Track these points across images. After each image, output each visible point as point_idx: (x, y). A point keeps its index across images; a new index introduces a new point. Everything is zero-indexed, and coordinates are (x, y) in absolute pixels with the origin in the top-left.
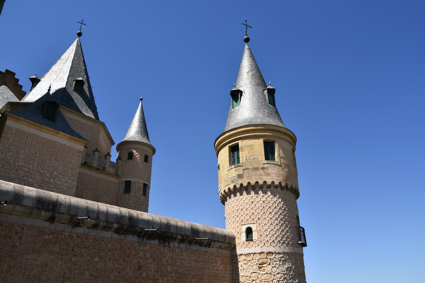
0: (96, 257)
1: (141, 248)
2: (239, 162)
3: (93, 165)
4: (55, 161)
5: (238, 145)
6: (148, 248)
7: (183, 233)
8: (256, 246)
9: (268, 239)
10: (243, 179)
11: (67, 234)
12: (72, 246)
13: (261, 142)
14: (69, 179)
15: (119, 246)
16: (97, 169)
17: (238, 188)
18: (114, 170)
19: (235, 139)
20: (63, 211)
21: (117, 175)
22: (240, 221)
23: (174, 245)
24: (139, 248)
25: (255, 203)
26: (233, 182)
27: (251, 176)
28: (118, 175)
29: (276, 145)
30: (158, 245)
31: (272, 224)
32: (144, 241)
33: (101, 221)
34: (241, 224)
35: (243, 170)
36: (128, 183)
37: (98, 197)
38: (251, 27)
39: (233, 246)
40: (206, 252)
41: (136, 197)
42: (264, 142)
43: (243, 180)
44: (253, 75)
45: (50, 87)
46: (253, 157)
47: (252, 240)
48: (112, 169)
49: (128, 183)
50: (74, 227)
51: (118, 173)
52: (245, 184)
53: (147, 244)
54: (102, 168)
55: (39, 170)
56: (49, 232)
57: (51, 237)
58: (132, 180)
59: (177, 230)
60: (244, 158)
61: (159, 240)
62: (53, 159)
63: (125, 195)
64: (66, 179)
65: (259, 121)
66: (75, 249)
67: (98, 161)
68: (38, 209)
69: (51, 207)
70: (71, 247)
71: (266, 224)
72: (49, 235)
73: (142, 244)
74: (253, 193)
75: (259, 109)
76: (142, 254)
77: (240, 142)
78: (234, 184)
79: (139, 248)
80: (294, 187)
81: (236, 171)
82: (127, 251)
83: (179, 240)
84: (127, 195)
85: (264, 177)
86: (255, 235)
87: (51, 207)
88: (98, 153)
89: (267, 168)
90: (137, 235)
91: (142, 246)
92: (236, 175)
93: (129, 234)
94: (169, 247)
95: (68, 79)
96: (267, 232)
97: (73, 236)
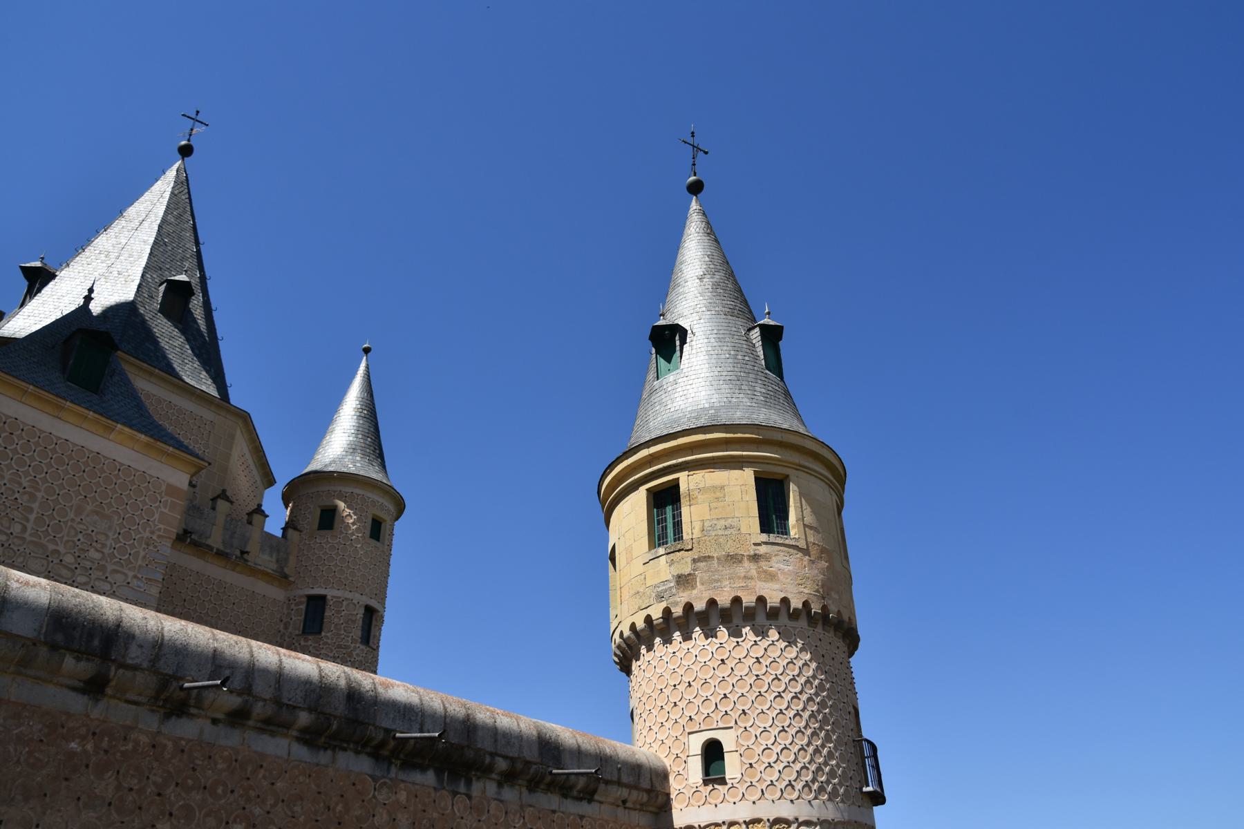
0: (235, 821)
1: (381, 798)
2: (678, 535)
3: (209, 542)
4: (96, 517)
5: (677, 486)
6: (402, 796)
7: (513, 753)
8: (737, 800)
9: (774, 778)
10: (693, 588)
11: (144, 739)
12: (160, 780)
13: (747, 477)
14: (135, 577)
16: (221, 554)
17: (679, 618)
18: (274, 559)
19: (669, 467)
20: (138, 661)
21: (282, 578)
22: (683, 721)
23: (484, 792)
24: (374, 797)
25: (730, 663)
26: (660, 597)
27: (717, 581)
28: (286, 577)
29: (793, 487)
30: (435, 788)
31: (783, 730)
32: (392, 774)
33: (257, 699)
34: (688, 730)
35: (694, 561)
36: (317, 604)
38: (706, 153)
39: (661, 799)
40: (582, 817)
41: (340, 647)
42: (758, 480)
43: (695, 592)
44: (716, 286)
45: (91, 290)
46: (722, 523)
47: (723, 781)
48: (266, 557)
49: (317, 604)
50: (168, 716)
51: (286, 570)
52: (699, 606)
53: (402, 785)
54: (238, 553)
55: (44, 541)
56: (83, 731)
57: (89, 747)
58: (330, 593)
59: (496, 741)
60: (697, 526)
61: (439, 773)
62: (89, 508)
63: (306, 640)
64: (126, 575)
65: (739, 417)
66: (168, 791)
68: (54, 647)
69: (96, 643)
70: (154, 783)
71: (765, 730)
72: (83, 738)
73: (385, 783)
74: (723, 632)
75: (737, 382)
76: (385, 817)
77: (682, 476)
78: (664, 605)
79: (374, 797)
80: (846, 618)
81: (672, 563)
82: (337, 804)
83: (502, 774)
85: (760, 584)
86: (732, 767)
87: (96, 643)
88: (228, 504)
89: (767, 558)
90: (369, 754)
91: (385, 790)
92: (670, 577)
93: (345, 750)
94: (469, 797)
95: (143, 276)
96: (769, 756)
97: (165, 746)
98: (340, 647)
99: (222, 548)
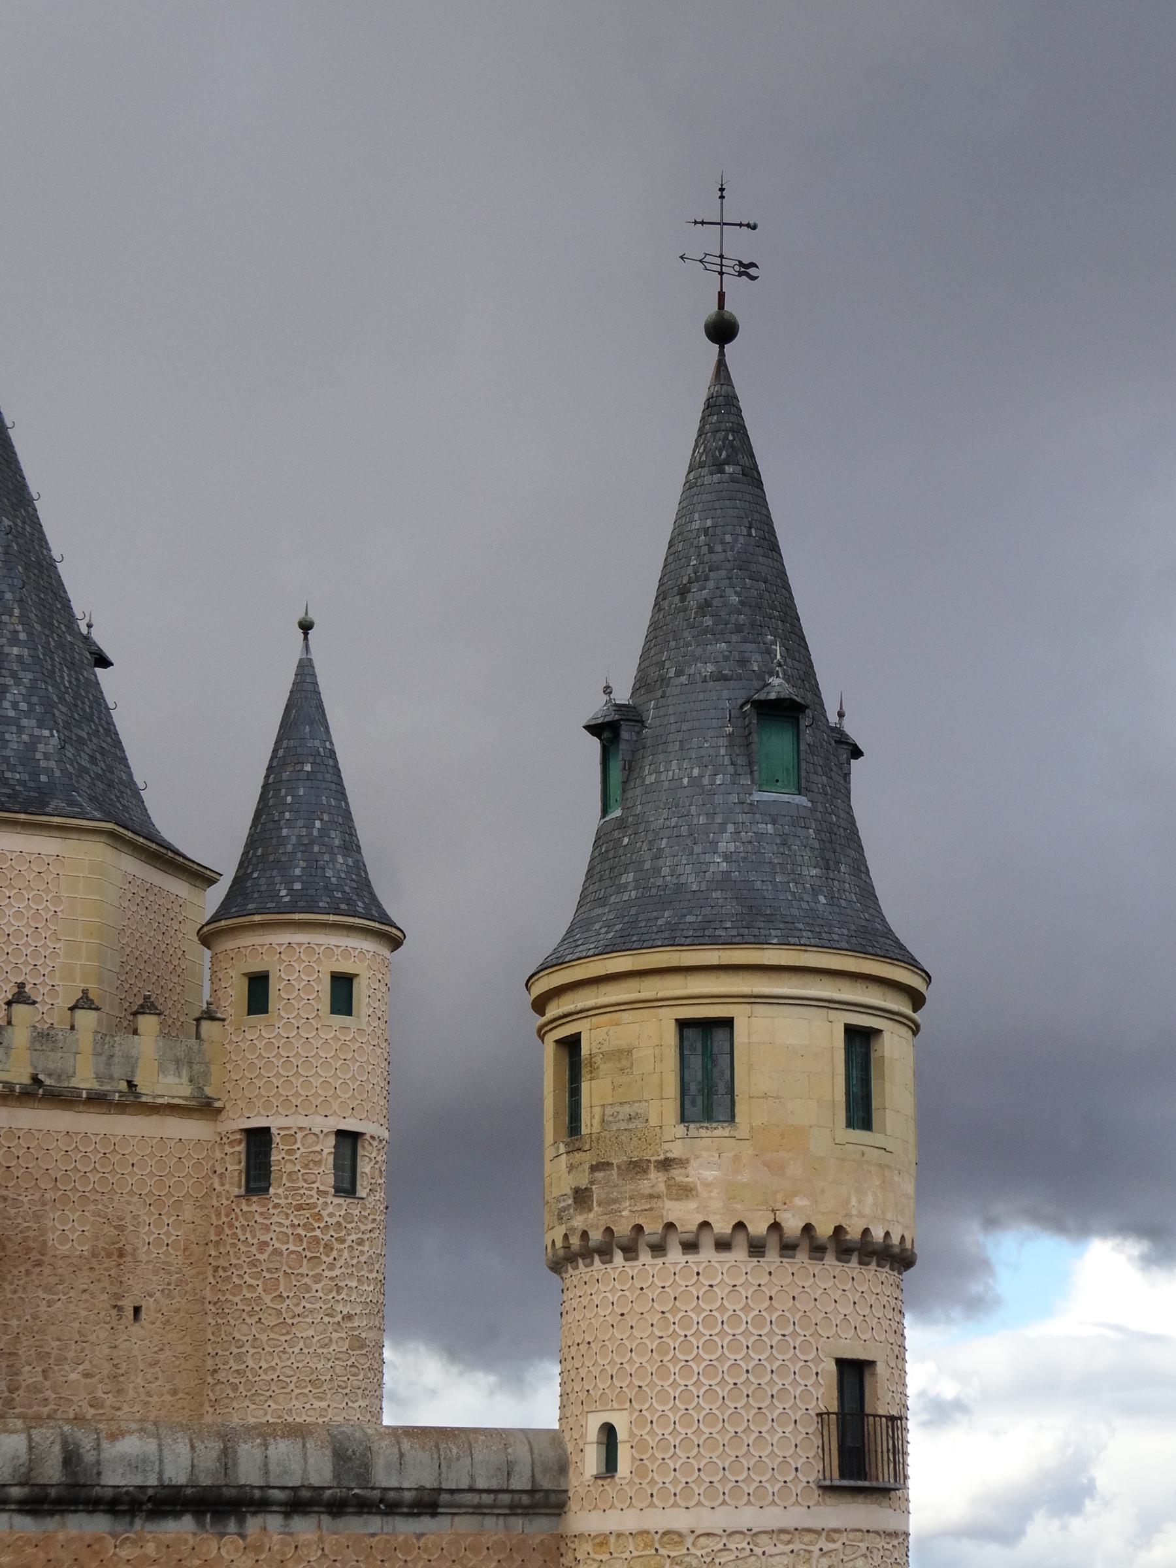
3: (75, 1082)
6: (150, 1549)
15: (42, 1555)
27: (615, 1201)
30: (195, 1534)
35: (593, 1169)
36: (258, 1141)
37: (121, 1228)
38: (754, 227)
40: (419, 1536)
41: (300, 1208)
43: (591, 1215)
46: (627, 1110)
48: (171, 1079)
52: (596, 1236)
54: (123, 1086)
60: (597, 1111)
61: (198, 1515)
67: (97, 1054)
73: (127, 1538)
81: (571, 1168)
84: (255, 1206)
85: (669, 1204)
88: (93, 1015)
89: (682, 1163)
90: (105, 1512)
92: (569, 1192)
98: (300, 1208)
99: (96, 1086)
